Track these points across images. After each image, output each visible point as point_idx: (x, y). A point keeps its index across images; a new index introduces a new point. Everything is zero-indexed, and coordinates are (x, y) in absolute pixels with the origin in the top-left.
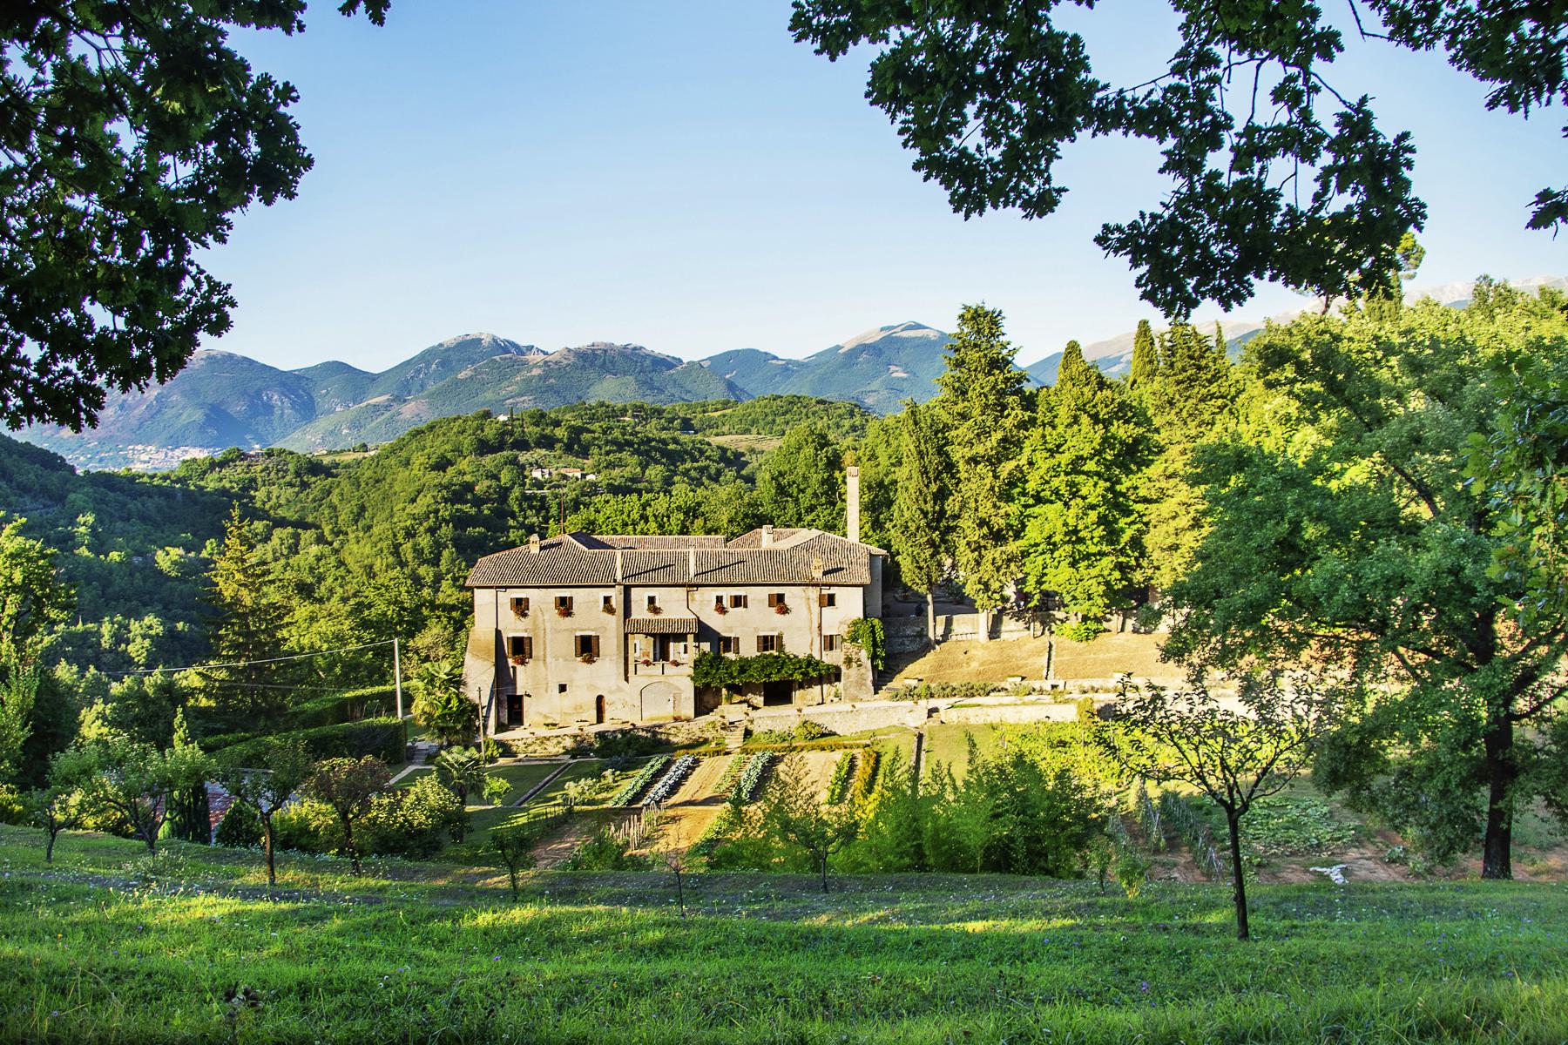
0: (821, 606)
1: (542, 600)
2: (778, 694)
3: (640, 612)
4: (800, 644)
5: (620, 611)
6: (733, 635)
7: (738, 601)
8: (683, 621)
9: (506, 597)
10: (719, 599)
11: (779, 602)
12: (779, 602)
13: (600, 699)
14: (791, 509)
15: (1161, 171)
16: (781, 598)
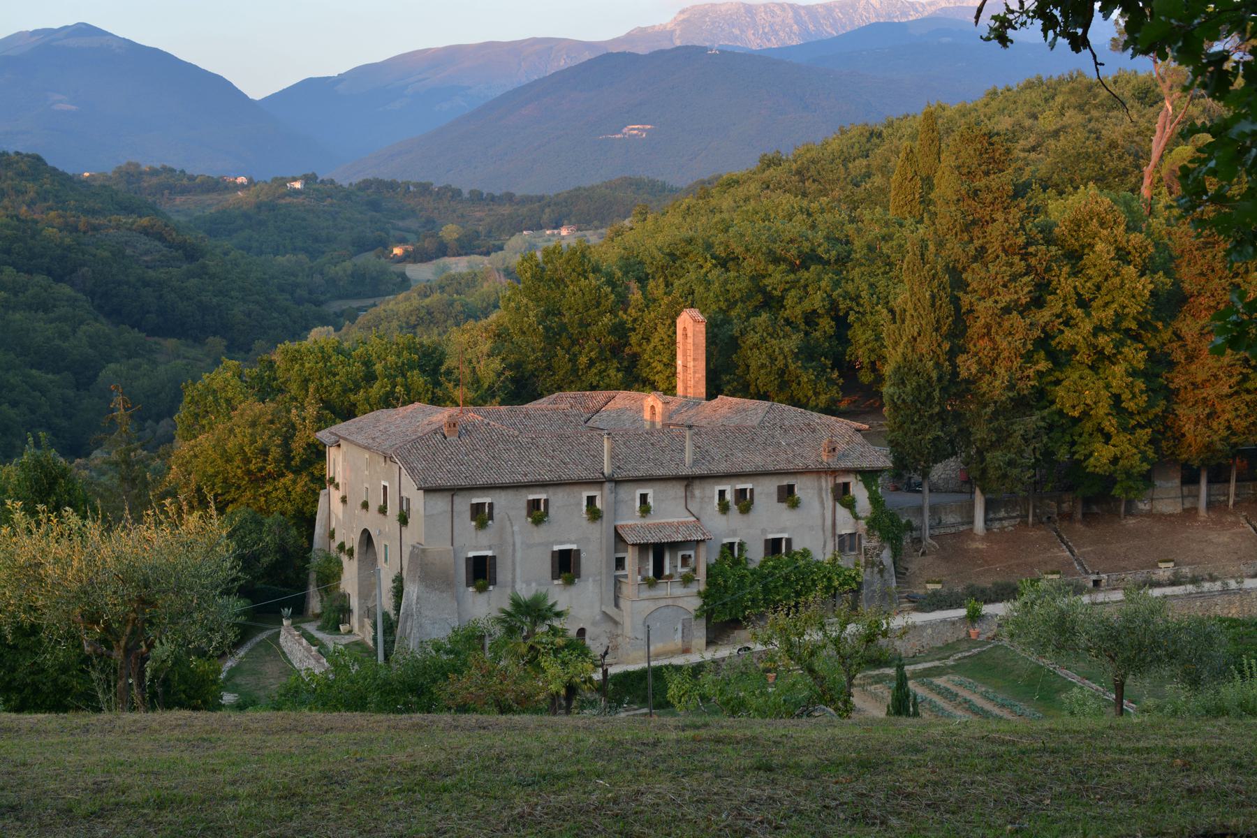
1: (510, 507)
6: (737, 540)
9: (464, 504)
10: (722, 493)
11: (787, 495)
12: (787, 495)
16: (790, 488)
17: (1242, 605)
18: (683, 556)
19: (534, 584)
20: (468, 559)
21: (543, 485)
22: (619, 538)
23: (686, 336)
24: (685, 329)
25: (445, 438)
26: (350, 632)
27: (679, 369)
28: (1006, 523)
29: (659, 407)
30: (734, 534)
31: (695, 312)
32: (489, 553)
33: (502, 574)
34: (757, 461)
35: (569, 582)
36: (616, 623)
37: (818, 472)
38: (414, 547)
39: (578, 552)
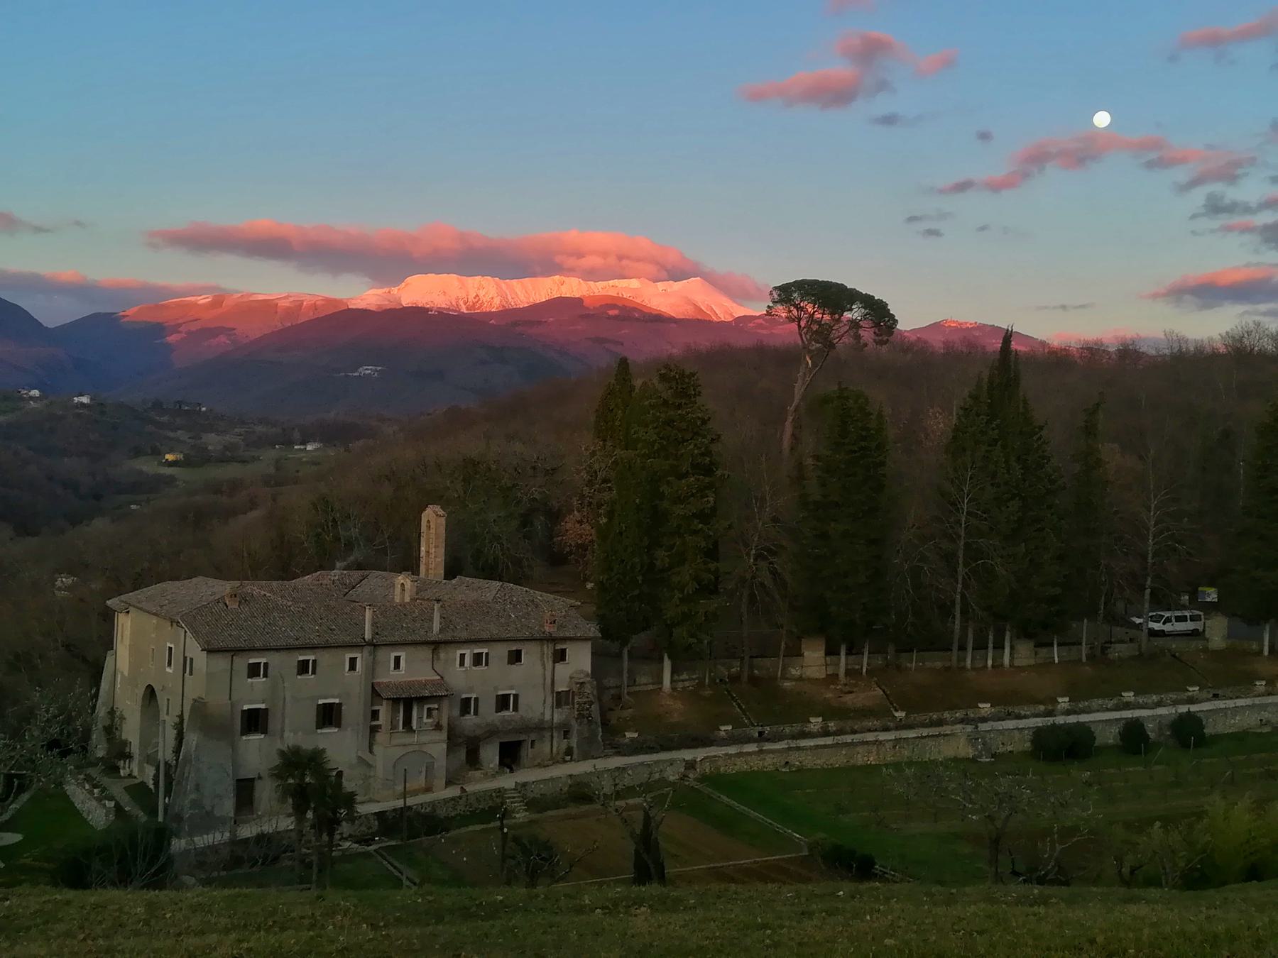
0: (554, 662)
6: (474, 696)
7: (477, 659)
9: (242, 663)
10: (463, 656)
16: (518, 653)
17: (878, 754)
18: (429, 710)
19: (300, 733)
20: (243, 711)
21: (313, 648)
22: (375, 694)
23: (429, 527)
24: (428, 522)
25: (227, 607)
26: (130, 776)
27: (423, 554)
28: (687, 684)
29: (408, 583)
30: (471, 690)
31: (438, 508)
32: (263, 706)
33: (273, 724)
34: (494, 630)
36: (369, 766)
37: (541, 640)
38: (195, 701)
39: (340, 705)
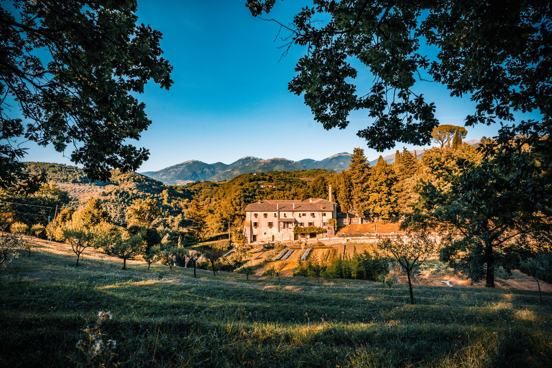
2: (313, 235)
3: (282, 217)
4: (318, 224)
5: (278, 217)
7: (304, 215)
8: (292, 219)
9: (253, 213)
10: (300, 214)
11: (313, 215)
12: (313, 215)
13: (273, 236)
14: (317, 194)
15: (369, 116)
16: (313, 214)
35: (271, 228)
